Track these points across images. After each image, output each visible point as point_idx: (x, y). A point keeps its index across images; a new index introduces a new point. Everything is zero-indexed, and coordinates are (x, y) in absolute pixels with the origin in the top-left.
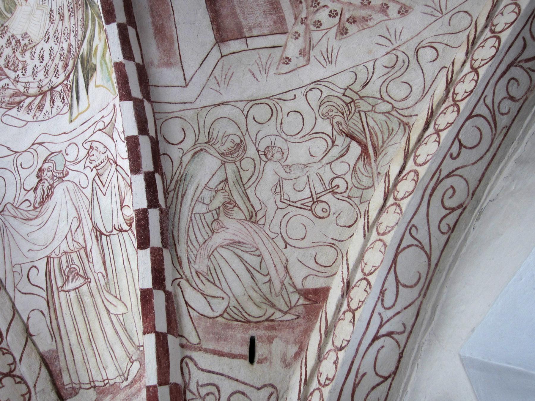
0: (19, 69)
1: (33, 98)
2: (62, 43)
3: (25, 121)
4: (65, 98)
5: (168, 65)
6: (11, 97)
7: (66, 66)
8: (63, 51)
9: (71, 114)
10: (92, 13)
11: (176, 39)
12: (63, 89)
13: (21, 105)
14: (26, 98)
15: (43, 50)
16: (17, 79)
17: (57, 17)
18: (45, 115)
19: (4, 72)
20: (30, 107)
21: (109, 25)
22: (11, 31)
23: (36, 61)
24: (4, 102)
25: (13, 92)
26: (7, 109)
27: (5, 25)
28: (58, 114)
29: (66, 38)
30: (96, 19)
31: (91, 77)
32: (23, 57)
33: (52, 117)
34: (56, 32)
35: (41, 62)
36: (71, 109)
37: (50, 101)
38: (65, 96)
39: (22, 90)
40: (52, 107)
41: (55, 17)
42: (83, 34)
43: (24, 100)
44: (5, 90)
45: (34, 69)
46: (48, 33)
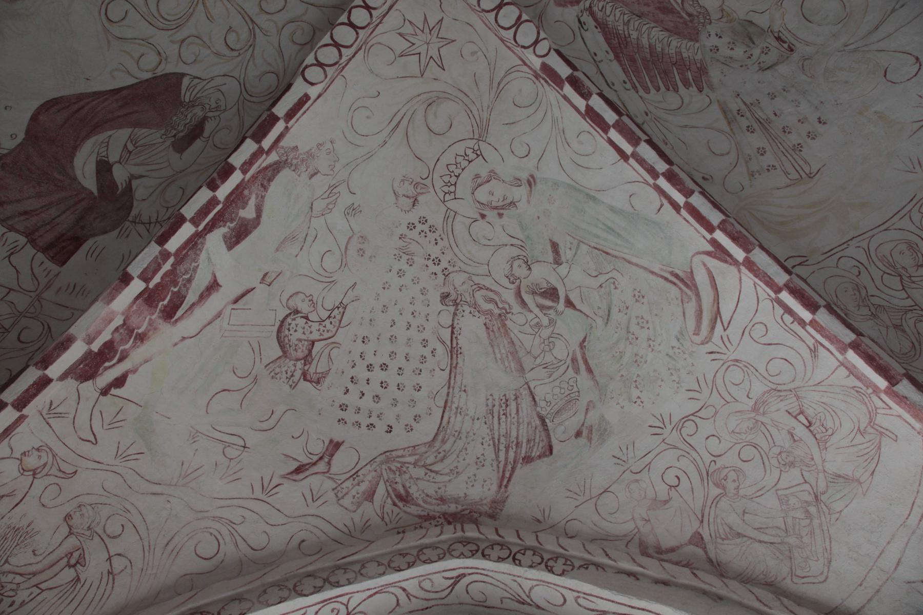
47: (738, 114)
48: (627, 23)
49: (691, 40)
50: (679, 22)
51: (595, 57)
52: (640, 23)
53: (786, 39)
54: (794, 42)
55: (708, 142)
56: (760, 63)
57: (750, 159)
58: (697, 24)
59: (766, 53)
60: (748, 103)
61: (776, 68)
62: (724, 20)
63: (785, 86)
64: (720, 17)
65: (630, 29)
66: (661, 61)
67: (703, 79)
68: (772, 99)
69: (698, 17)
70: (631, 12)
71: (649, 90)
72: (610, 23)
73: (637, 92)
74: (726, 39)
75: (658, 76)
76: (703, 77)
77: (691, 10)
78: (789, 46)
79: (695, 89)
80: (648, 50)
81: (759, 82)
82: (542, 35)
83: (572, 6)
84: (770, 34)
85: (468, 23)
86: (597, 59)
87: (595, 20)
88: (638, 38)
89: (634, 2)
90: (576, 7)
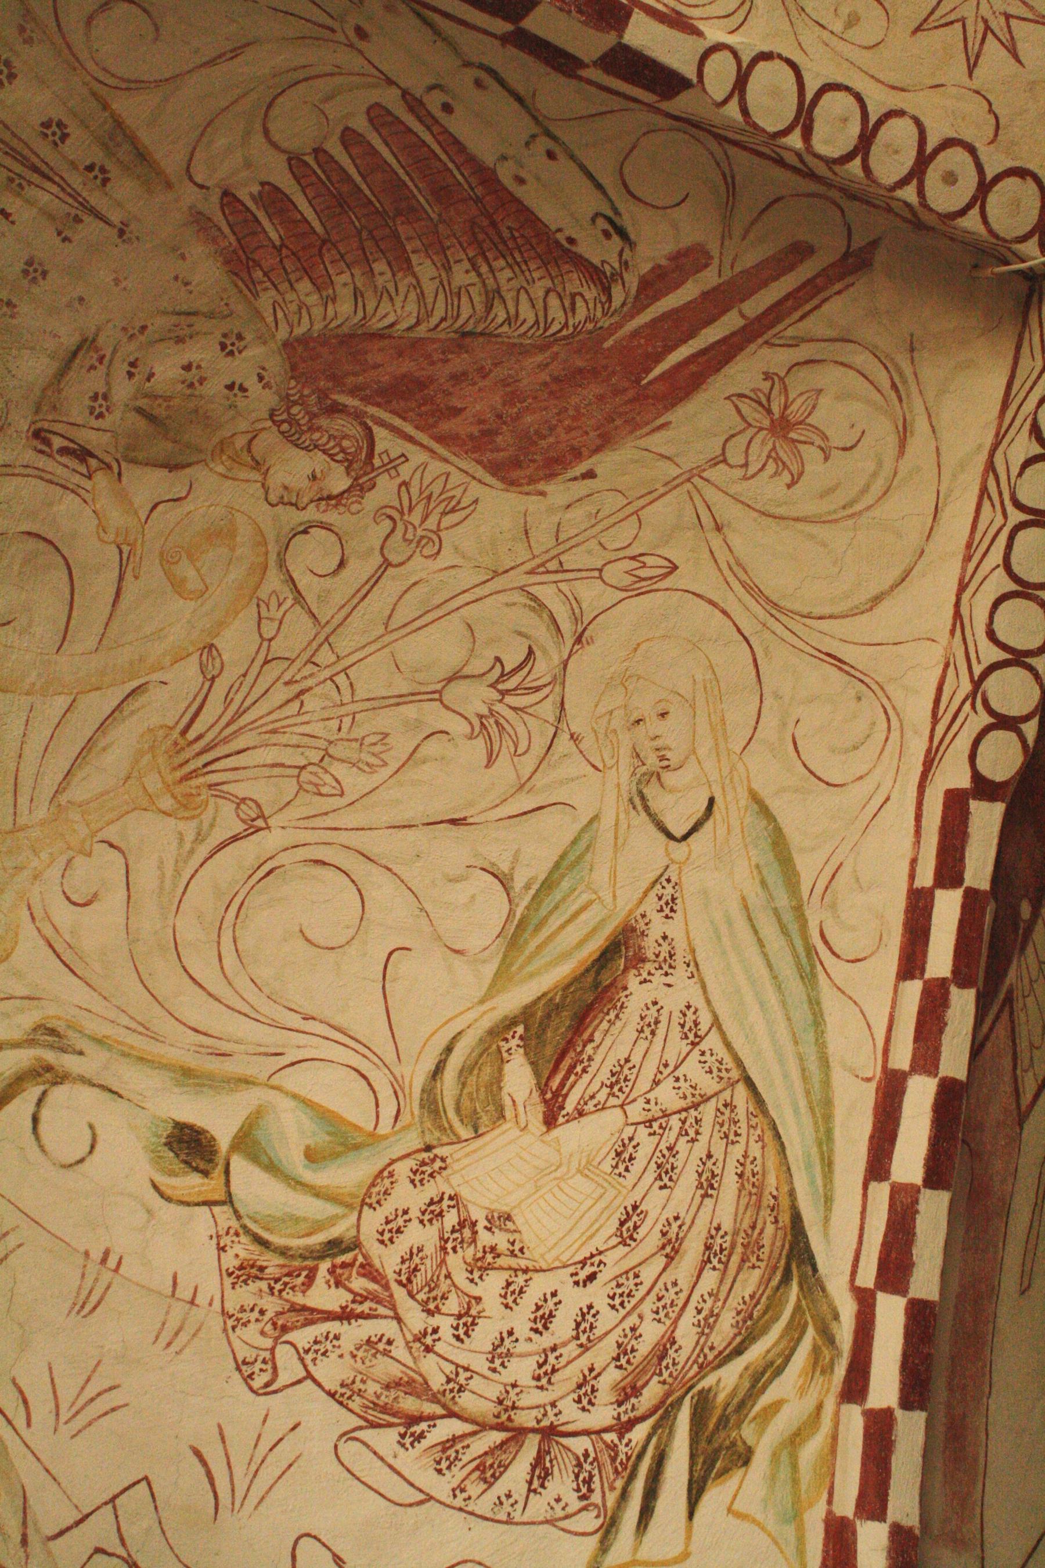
0: (444, 1309)
1: (469, 1428)
2: (641, 1317)
3: (421, 1491)
4: (596, 1484)
5: (958, 1543)
6: (387, 1387)
7: (628, 1392)
8: (633, 1342)
9: (604, 1547)
10: (798, 1308)
11: (981, 1470)
12: (592, 1455)
13: (417, 1429)
14: (443, 1417)
15: (556, 1300)
16: (429, 1340)
17: (650, 1239)
18: (501, 1503)
19: (391, 1296)
20: (451, 1453)
21: (907, 1413)
22: (456, 1180)
23: (521, 1320)
24: (360, 1393)
25: (400, 1375)
26: (366, 1420)
27: (436, 1151)
28: (547, 1522)
29: (662, 1314)
30: (810, 1332)
31: (720, 1475)
32: (472, 1281)
33: (525, 1524)
34: (631, 1275)
35: (536, 1331)
36: (608, 1532)
37: (534, 1468)
38: (596, 1479)
39: (437, 1382)
40: (535, 1491)
41: (642, 1231)
42: (739, 1339)
43: (432, 1418)
44: (374, 1356)
45: (502, 1339)
46: (596, 1260)
47: (103, 170)
48: (493, 296)
49: (304, 340)
50: (355, 374)
51: (551, 145)
52: (458, 316)
53: (64, 460)
54: (42, 462)
55: (157, 30)
56: (101, 360)
57: (22, 29)
58: (306, 392)
59: (95, 398)
60: (87, 219)
61: (55, 365)
62: (241, 442)
63: (13, 317)
64: (255, 442)
65: (479, 285)
66: (365, 234)
67: (232, 239)
68: (30, 263)
69: (313, 416)
70: (490, 335)
71: (371, 121)
72: (536, 275)
73: (405, 93)
74: (214, 387)
75: (358, 179)
76: (235, 243)
77: (340, 424)
78: (48, 443)
79: (243, 195)
80: (409, 248)
81: (81, 299)
82: (733, 110)
83: (657, 267)
84: (108, 459)
85: (903, 90)
86: (543, 144)
87: (581, 263)
88: (448, 268)
89: (496, 365)
90: (645, 268)
